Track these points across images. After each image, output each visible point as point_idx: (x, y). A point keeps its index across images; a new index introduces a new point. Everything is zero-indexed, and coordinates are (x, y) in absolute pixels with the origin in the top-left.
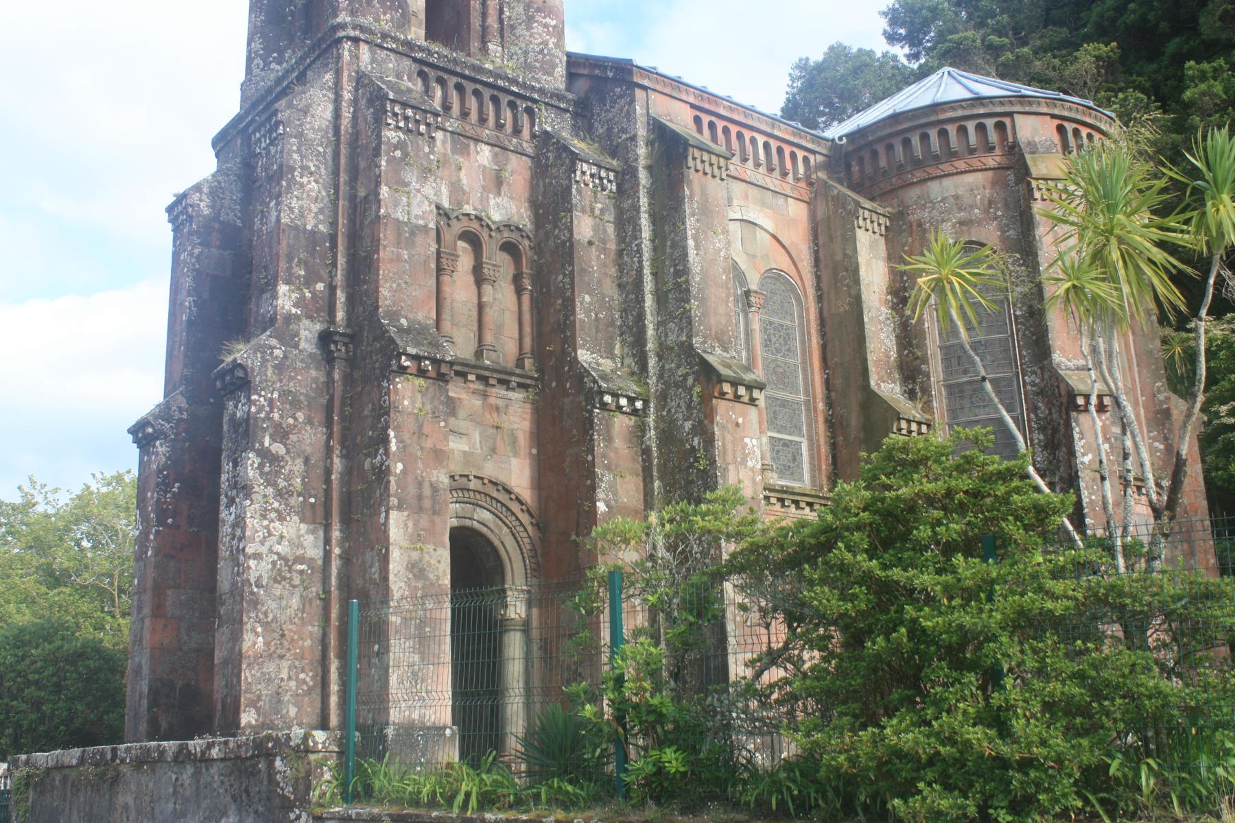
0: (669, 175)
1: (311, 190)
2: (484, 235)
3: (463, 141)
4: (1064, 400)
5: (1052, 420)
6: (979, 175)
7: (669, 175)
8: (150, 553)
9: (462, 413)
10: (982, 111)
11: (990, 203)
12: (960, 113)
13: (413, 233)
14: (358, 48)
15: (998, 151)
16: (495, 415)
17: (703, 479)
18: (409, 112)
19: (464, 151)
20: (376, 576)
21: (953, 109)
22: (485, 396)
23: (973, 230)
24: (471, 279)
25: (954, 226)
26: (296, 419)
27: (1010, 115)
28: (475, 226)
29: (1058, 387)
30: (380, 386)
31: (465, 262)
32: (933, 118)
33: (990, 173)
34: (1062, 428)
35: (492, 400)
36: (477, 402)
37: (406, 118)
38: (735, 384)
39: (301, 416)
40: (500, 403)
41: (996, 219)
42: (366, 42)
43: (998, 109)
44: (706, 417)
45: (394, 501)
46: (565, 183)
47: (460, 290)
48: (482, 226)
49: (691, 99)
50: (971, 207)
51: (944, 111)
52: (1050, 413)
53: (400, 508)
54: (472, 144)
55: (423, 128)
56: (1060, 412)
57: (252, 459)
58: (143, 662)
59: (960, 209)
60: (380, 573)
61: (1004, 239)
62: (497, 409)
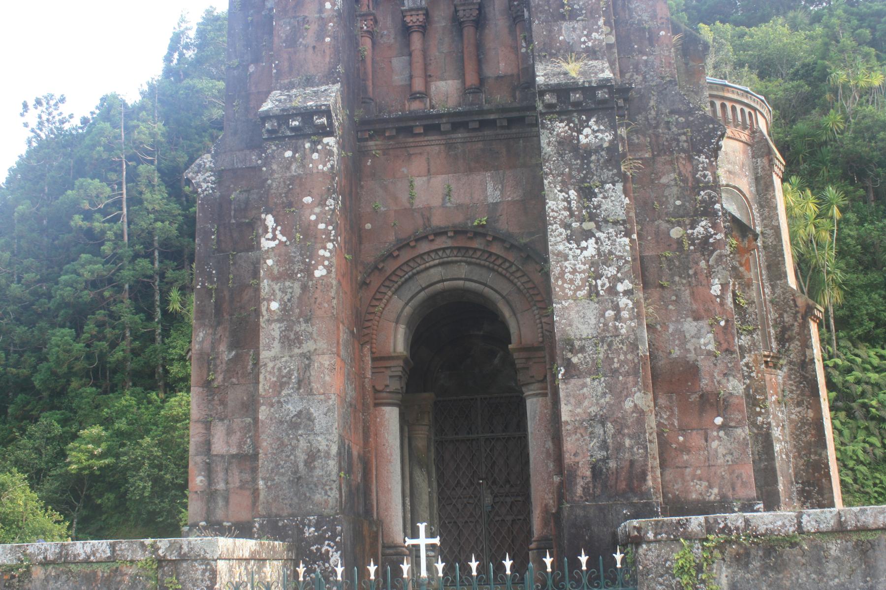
0: (686, 64)
4: (802, 310)
5: (783, 322)
6: (737, 142)
7: (686, 64)
8: (320, 272)
10: (746, 101)
11: (743, 164)
12: (735, 97)
15: (746, 132)
17: (740, 314)
20: (711, 347)
21: (733, 92)
23: (736, 179)
25: (726, 172)
27: (755, 109)
29: (794, 300)
30: (690, 159)
32: (721, 94)
33: (741, 144)
34: (796, 329)
41: (746, 176)
43: (753, 104)
44: (741, 265)
50: (735, 163)
51: (728, 91)
52: (781, 316)
56: (795, 318)
58: (316, 412)
59: (729, 163)
60: (719, 344)
61: (751, 192)
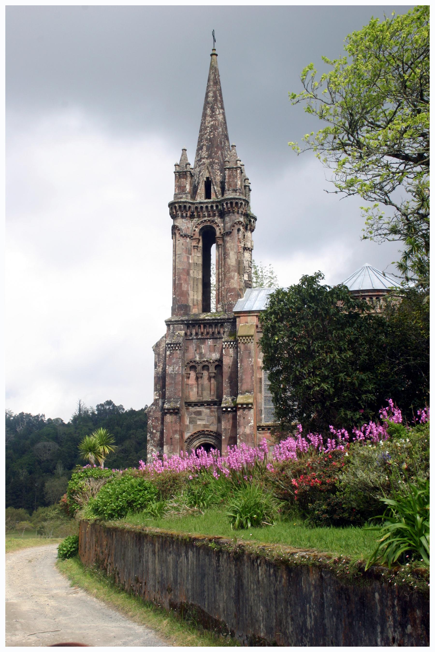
2: (210, 365)
3: (203, 340)
9: (203, 414)
13: (175, 376)
19: (203, 343)
22: (210, 408)
28: (206, 363)
35: (213, 409)
36: (208, 411)
37: (172, 347)
38: (242, 404)
45: (165, 443)
47: (205, 381)
49: (256, 314)
53: (166, 445)
57: (149, 435)
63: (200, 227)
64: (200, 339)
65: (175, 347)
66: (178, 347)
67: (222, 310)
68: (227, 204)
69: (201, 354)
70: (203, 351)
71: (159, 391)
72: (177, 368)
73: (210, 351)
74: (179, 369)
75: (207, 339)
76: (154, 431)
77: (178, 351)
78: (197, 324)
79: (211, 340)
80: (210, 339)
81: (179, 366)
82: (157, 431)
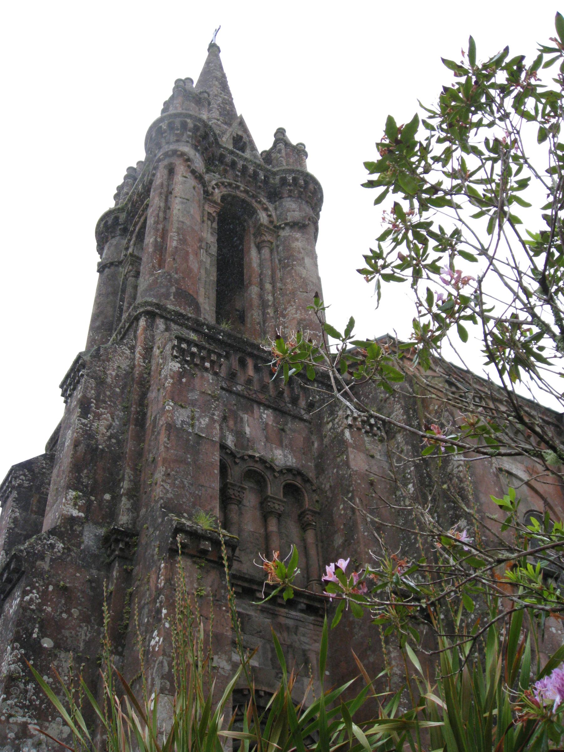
1: (105, 419)
2: (268, 475)
14: (153, 321)
16: (285, 634)
18: (194, 349)
19: (249, 410)
24: (258, 514)
26: (70, 615)
28: (258, 467)
31: (250, 500)
35: (282, 620)
37: (193, 355)
39: (75, 612)
40: (290, 623)
42: (162, 317)
46: (339, 430)
48: (266, 467)
54: (255, 406)
55: (207, 365)
62: (288, 628)
63: (225, 191)
64: (238, 394)
65: (203, 359)
66: (212, 363)
67: (189, 410)
68: (294, 179)
69: (239, 434)
70: (247, 430)
71: (85, 494)
72: (204, 421)
73: (267, 439)
74: (209, 426)
75: (259, 403)
76: (47, 643)
77: (210, 377)
78: (238, 350)
79: (269, 412)
80: (267, 407)
81: (212, 420)
82: (57, 646)
